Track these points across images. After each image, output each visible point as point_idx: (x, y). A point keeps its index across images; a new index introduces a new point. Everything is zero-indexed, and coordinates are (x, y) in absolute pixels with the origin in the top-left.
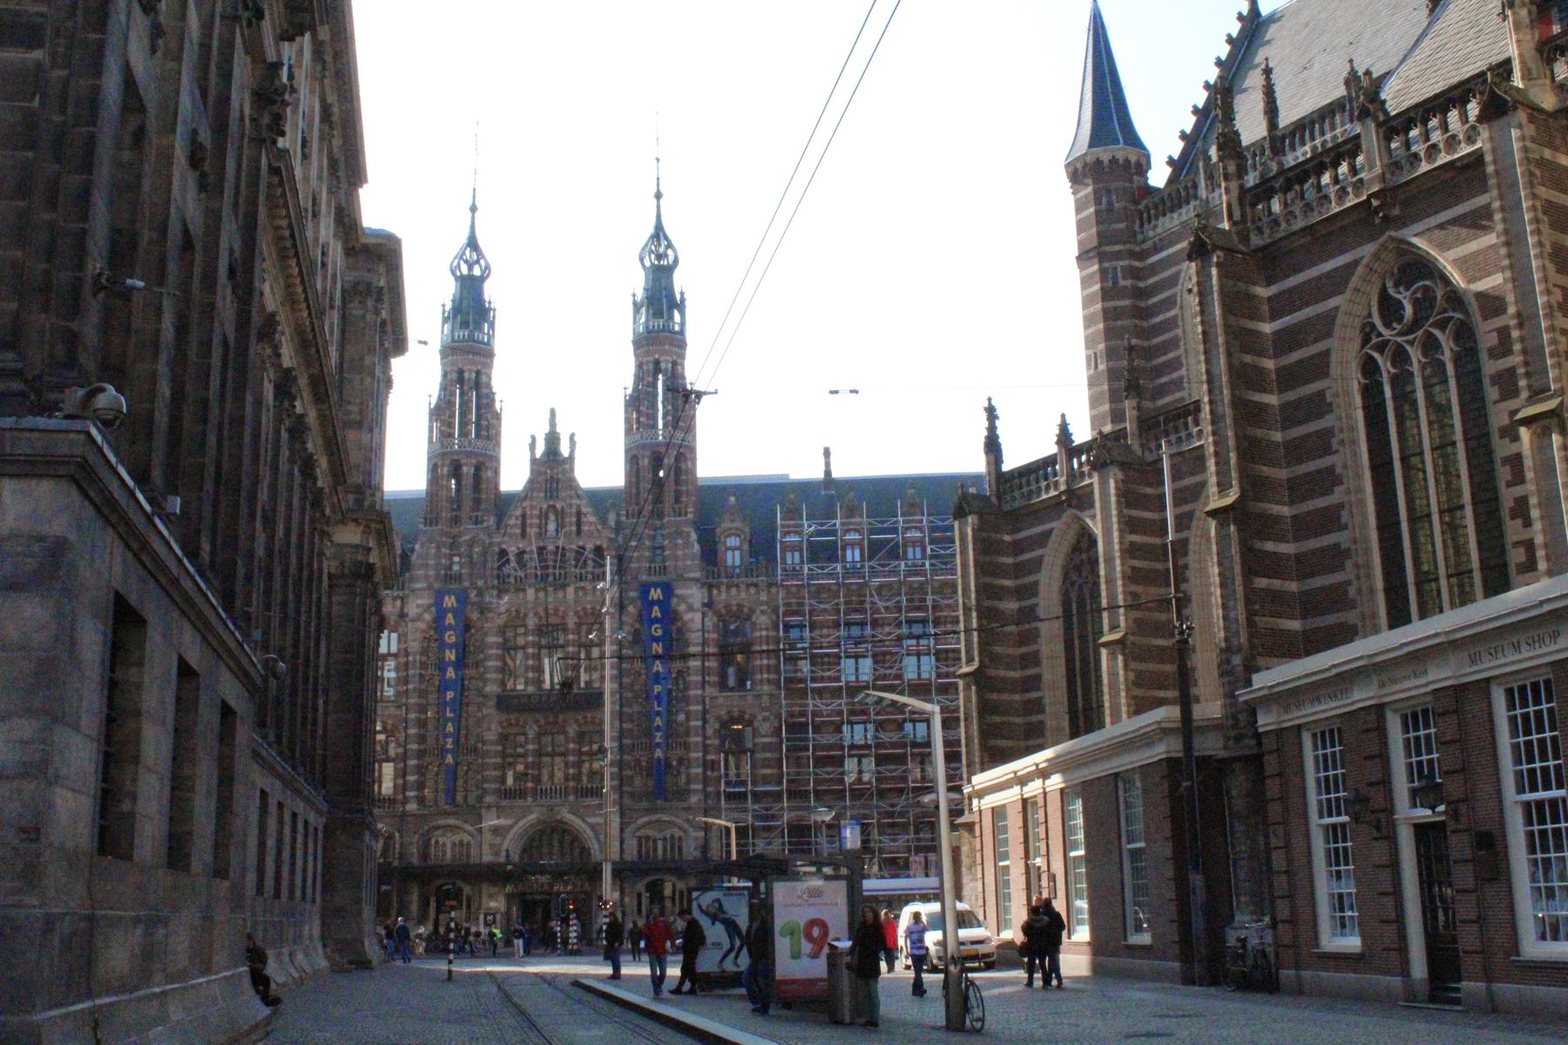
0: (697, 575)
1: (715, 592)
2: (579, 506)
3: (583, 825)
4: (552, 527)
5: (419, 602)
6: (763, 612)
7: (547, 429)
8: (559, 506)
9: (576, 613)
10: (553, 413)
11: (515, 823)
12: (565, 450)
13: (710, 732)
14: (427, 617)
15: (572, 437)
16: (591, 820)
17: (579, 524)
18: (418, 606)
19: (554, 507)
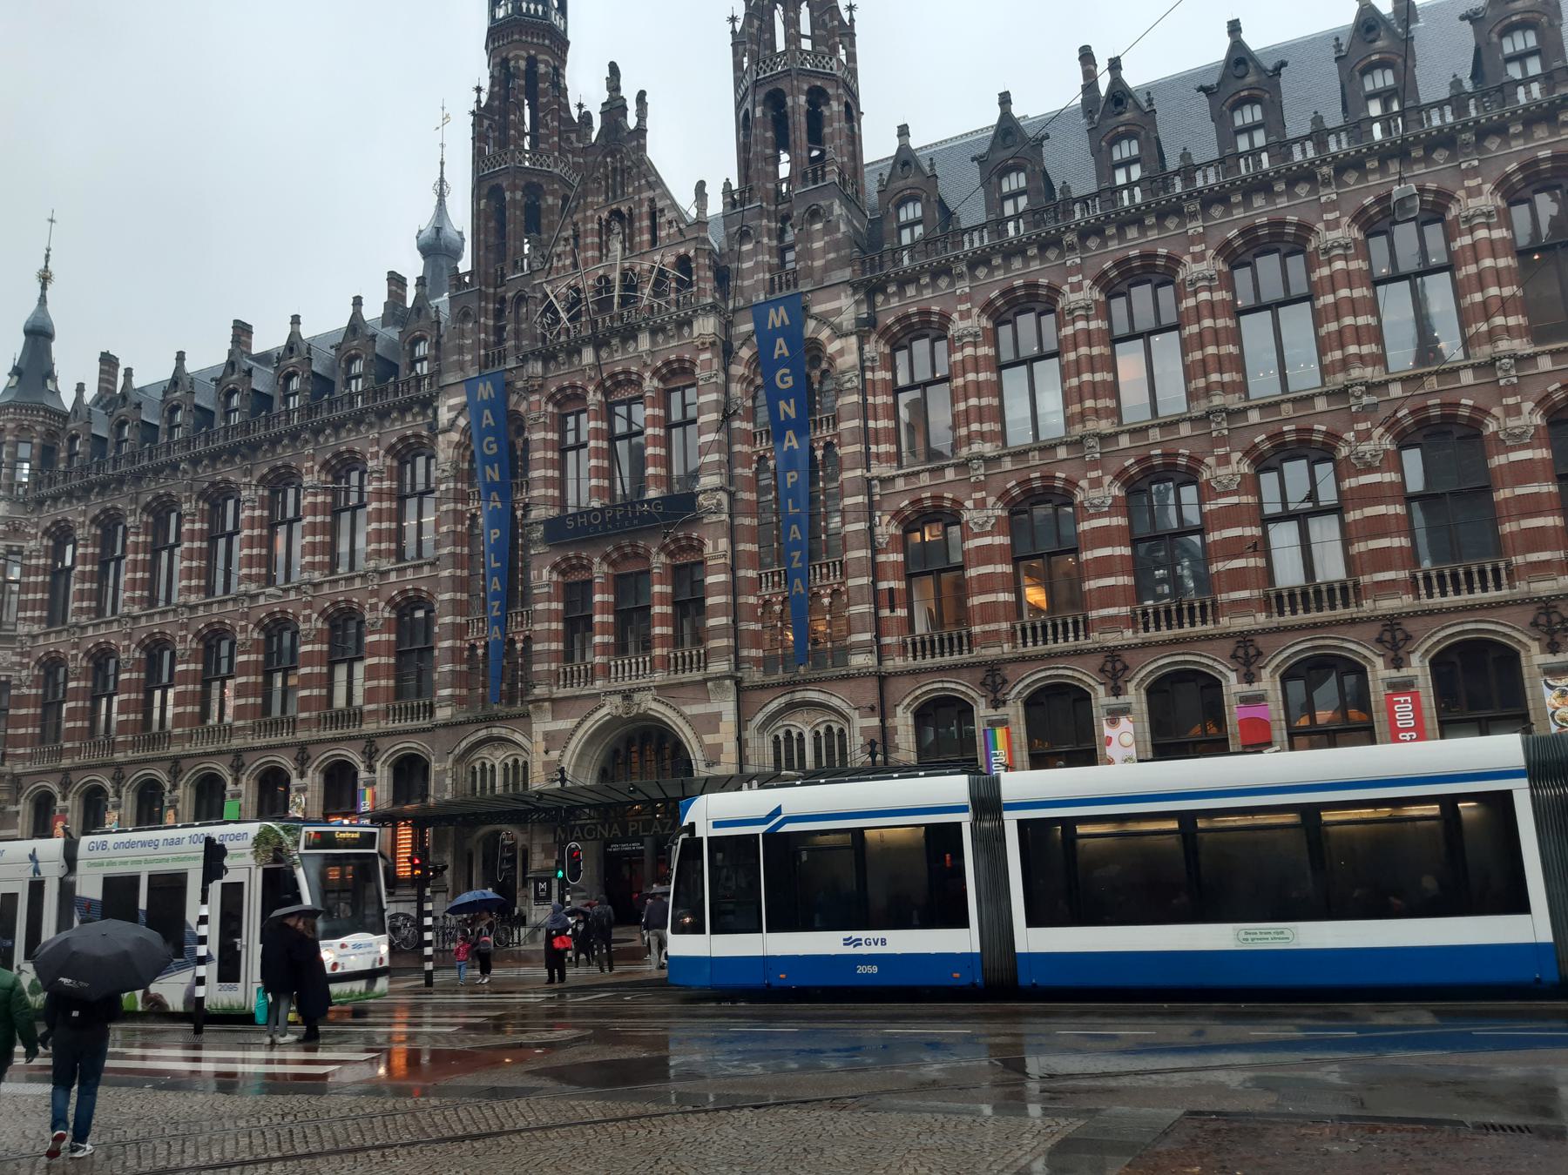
0: (847, 274)
1: (880, 299)
2: (652, 200)
3: (680, 722)
4: (616, 247)
5: (453, 401)
6: (965, 315)
7: (605, 96)
8: (624, 209)
9: (656, 372)
10: (614, 69)
11: (579, 725)
12: (632, 121)
13: (882, 540)
14: (462, 422)
15: (641, 96)
16: (689, 710)
17: (654, 228)
18: (450, 409)
19: (617, 214)
